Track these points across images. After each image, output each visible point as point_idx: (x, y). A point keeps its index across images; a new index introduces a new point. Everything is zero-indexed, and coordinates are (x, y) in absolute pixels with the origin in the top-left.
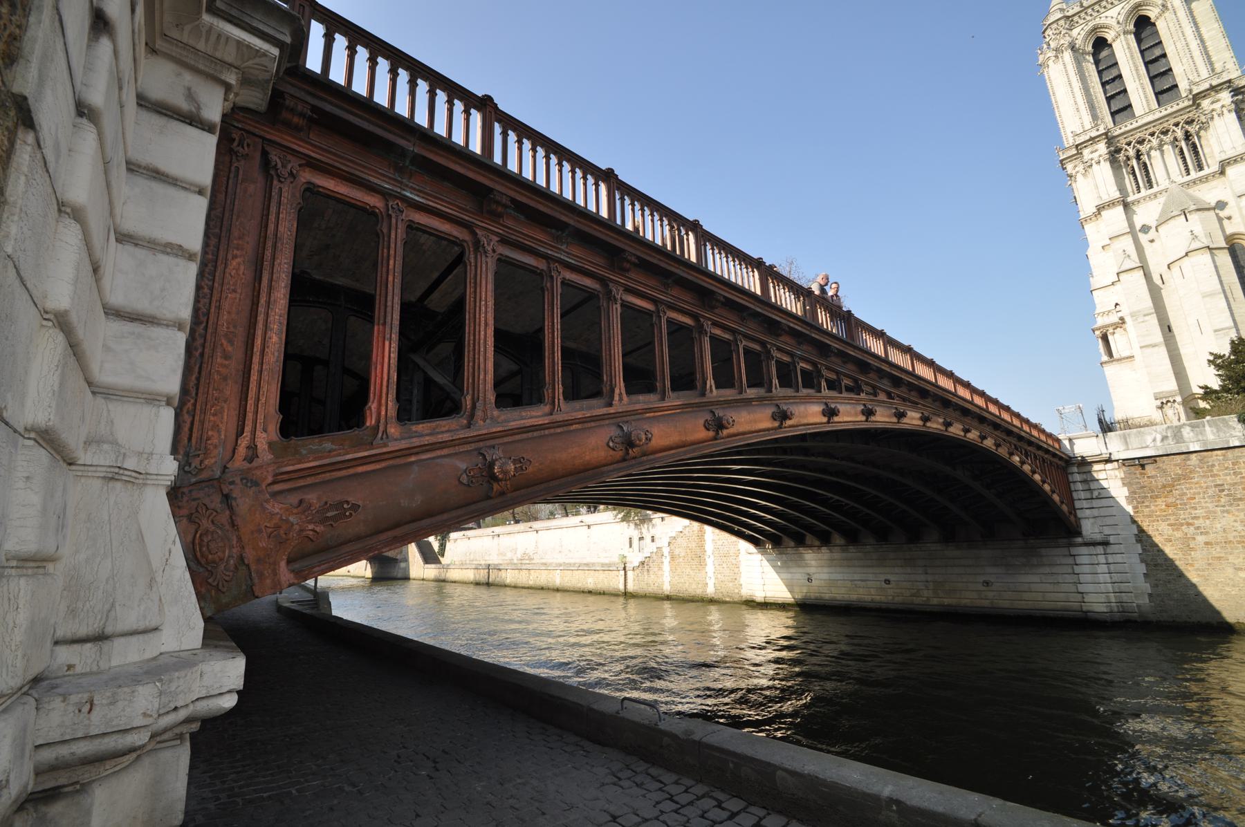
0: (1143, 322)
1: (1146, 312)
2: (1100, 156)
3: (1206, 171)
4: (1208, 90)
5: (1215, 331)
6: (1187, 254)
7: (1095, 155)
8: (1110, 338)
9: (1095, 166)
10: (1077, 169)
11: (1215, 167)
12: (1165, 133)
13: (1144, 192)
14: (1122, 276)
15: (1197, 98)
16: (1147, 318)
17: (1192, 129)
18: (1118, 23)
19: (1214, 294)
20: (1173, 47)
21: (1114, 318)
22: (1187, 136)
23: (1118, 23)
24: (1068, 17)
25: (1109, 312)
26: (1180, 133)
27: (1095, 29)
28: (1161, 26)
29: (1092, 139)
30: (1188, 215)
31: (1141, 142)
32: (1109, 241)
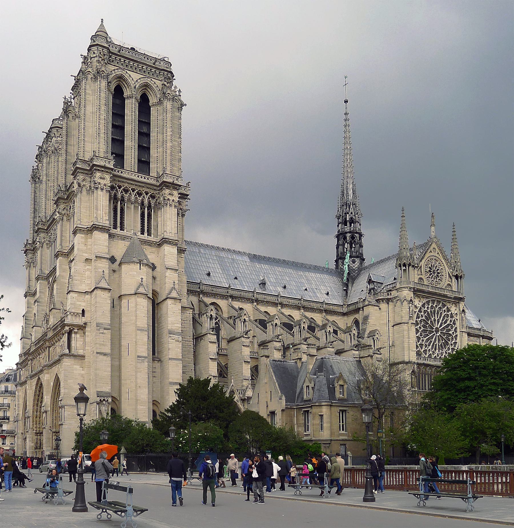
0: (102, 333)
1: (106, 327)
2: (105, 185)
3: (152, 238)
4: (170, 183)
5: (138, 357)
6: (136, 294)
7: (102, 182)
8: (73, 335)
9: (99, 190)
10: (84, 183)
11: (158, 239)
12: (140, 194)
13: (118, 231)
14: (98, 292)
15: (165, 185)
16: (105, 331)
17: (153, 202)
18: (135, 87)
19: (143, 330)
20: (156, 134)
21: (80, 321)
22: (149, 207)
23: (135, 87)
24: (110, 52)
25: (78, 314)
26: (146, 202)
27: (120, 78)
28: (153, 111)
29: (104, 167)
30: (141, 265)
31: (126, 191)
32: (94, 258)
